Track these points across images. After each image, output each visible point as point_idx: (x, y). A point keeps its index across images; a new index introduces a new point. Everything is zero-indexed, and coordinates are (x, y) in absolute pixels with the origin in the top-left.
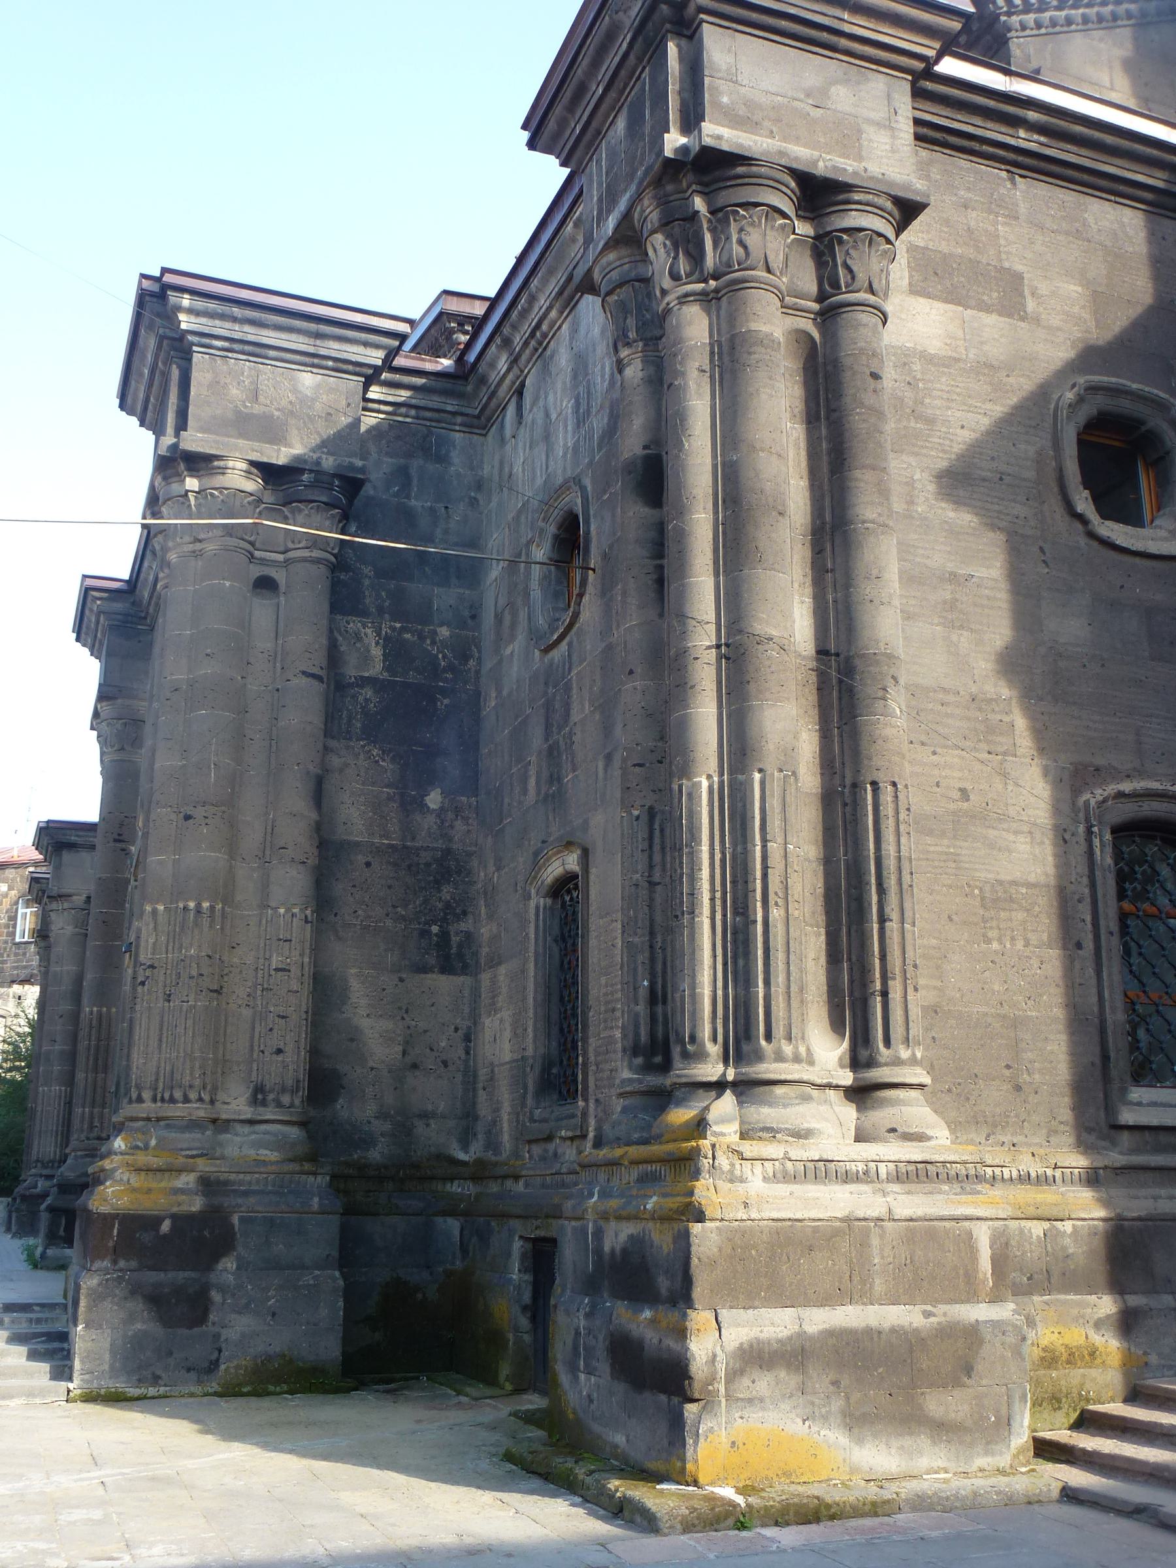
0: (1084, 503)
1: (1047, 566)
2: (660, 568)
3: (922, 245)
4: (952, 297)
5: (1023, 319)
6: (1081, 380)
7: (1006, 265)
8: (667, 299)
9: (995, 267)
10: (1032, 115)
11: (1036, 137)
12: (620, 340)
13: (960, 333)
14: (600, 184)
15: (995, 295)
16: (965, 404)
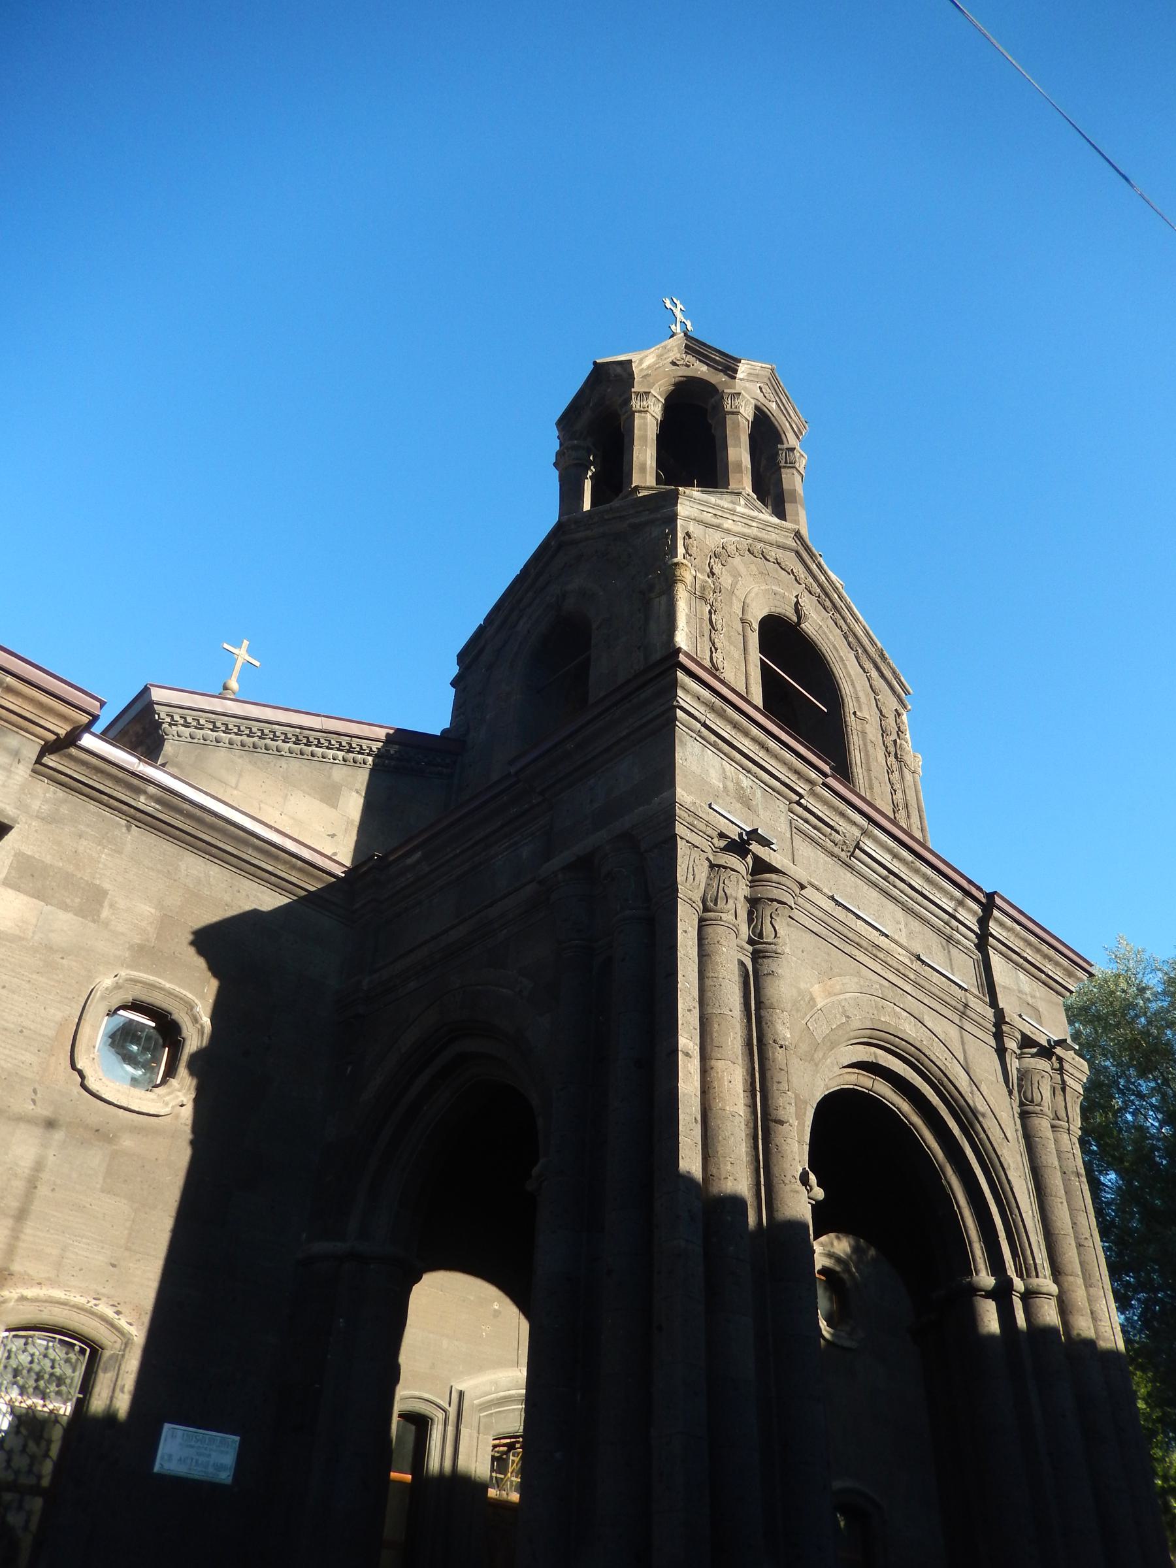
1: (35, 1104)
3: (29, 853)
4: (38, 895)
5: (94, 921)
6: (124, 973)
7: (98, 882)
9: (87, 881)
10: (151, 789)
11: (153, 804)
13: (34, 921)
15: (77, 900)
16: (13, 971)
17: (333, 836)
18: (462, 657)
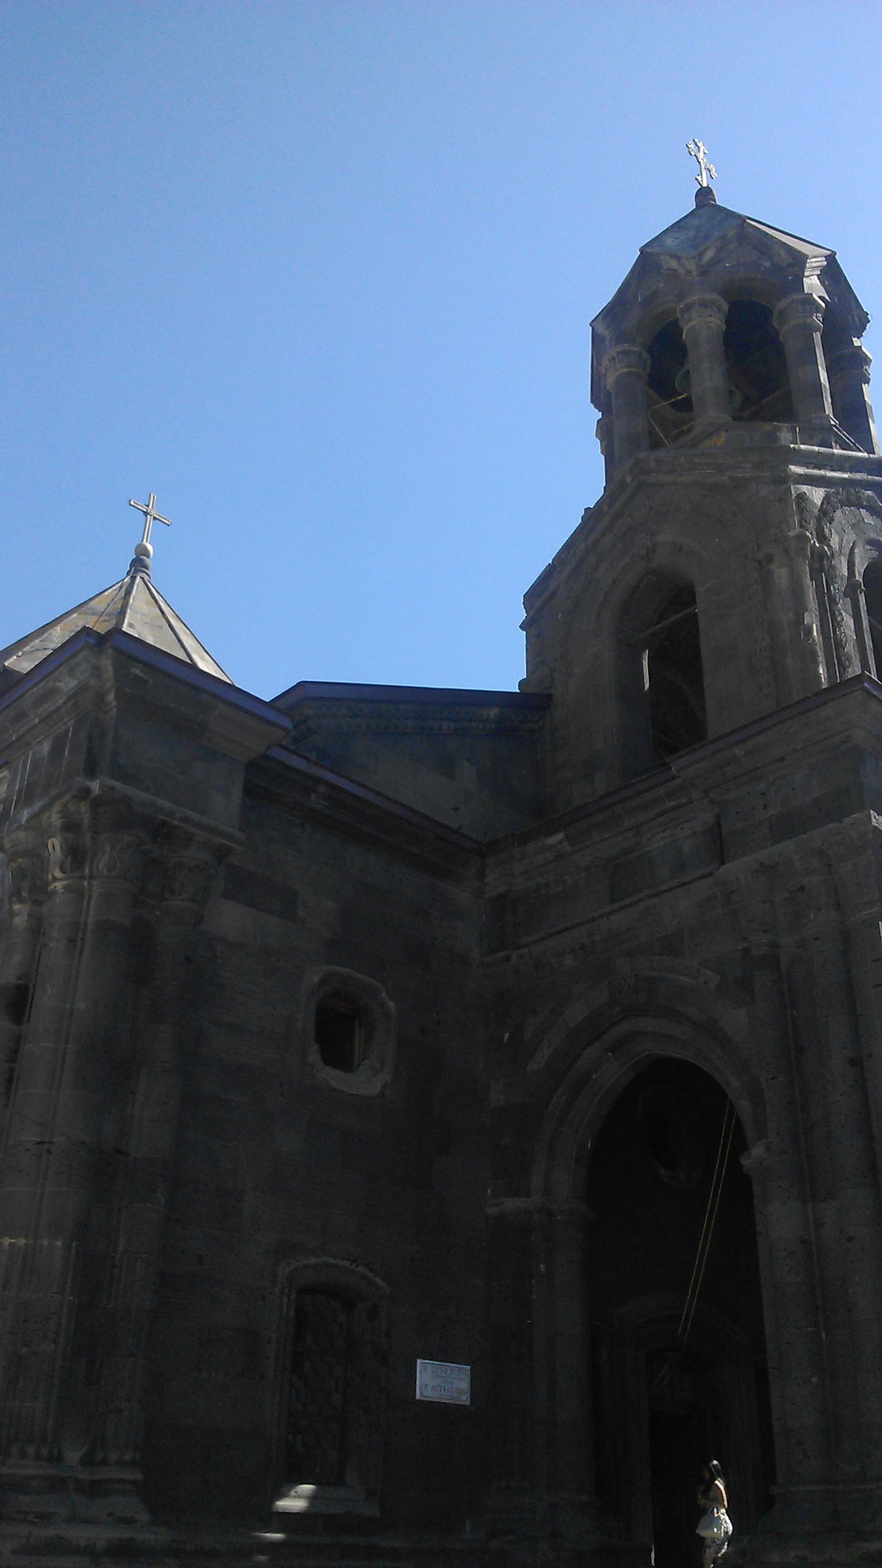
0: (314, 1055)
2: (12, 1070)
8: (55, 884)
12: (16, 893)
14: (22, 781)
17: (456, 809)
18: (530, 599)
